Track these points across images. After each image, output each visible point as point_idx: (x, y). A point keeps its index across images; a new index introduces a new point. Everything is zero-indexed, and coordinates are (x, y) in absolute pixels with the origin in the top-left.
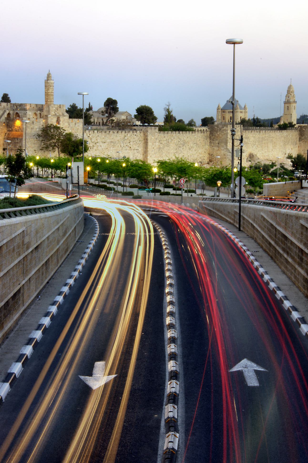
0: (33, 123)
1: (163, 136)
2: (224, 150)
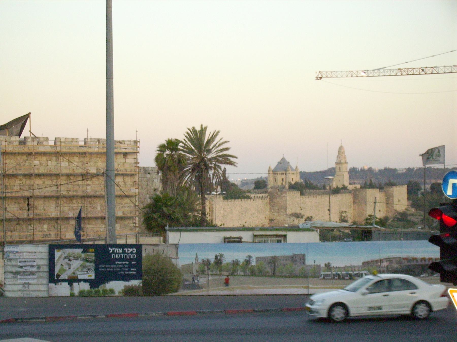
1: (227, 204)
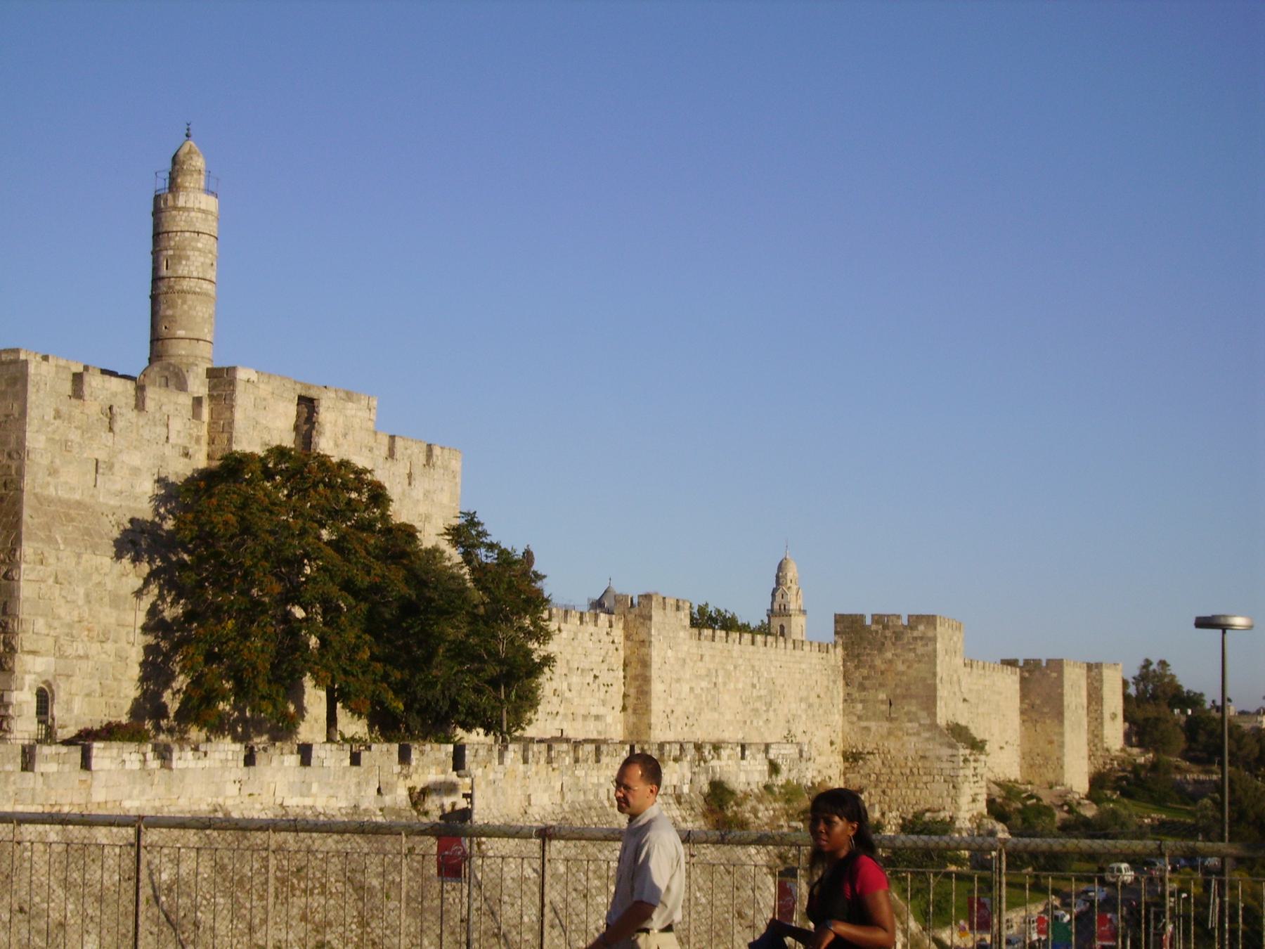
0: (111, 420)
1: (694, 650)
2: (918, 734)
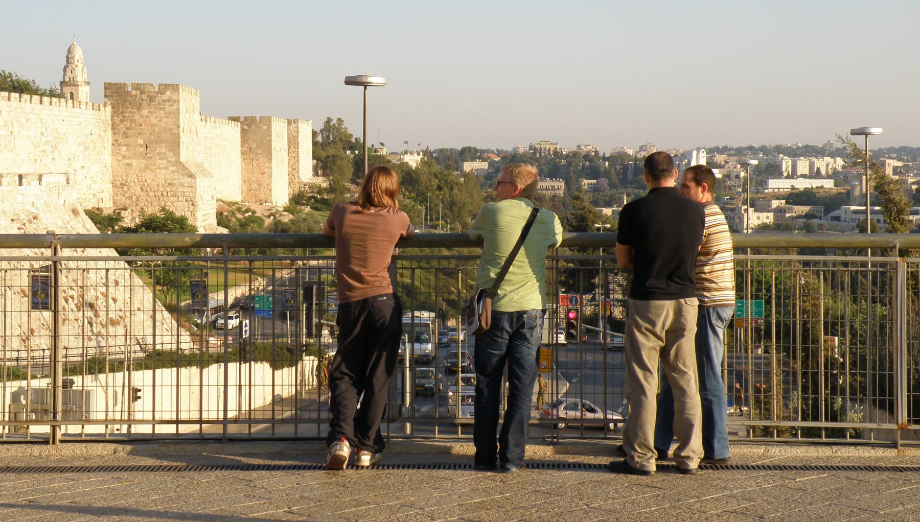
2: (167, 168)
